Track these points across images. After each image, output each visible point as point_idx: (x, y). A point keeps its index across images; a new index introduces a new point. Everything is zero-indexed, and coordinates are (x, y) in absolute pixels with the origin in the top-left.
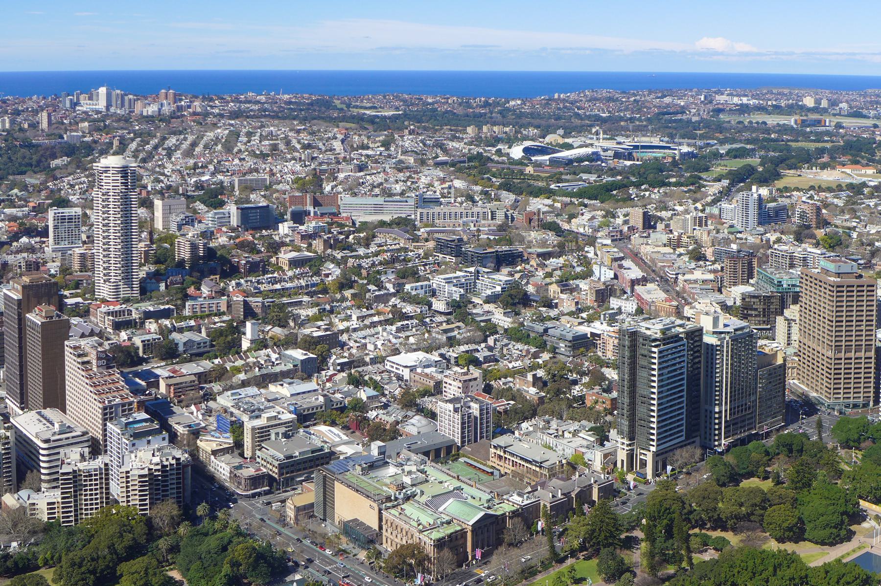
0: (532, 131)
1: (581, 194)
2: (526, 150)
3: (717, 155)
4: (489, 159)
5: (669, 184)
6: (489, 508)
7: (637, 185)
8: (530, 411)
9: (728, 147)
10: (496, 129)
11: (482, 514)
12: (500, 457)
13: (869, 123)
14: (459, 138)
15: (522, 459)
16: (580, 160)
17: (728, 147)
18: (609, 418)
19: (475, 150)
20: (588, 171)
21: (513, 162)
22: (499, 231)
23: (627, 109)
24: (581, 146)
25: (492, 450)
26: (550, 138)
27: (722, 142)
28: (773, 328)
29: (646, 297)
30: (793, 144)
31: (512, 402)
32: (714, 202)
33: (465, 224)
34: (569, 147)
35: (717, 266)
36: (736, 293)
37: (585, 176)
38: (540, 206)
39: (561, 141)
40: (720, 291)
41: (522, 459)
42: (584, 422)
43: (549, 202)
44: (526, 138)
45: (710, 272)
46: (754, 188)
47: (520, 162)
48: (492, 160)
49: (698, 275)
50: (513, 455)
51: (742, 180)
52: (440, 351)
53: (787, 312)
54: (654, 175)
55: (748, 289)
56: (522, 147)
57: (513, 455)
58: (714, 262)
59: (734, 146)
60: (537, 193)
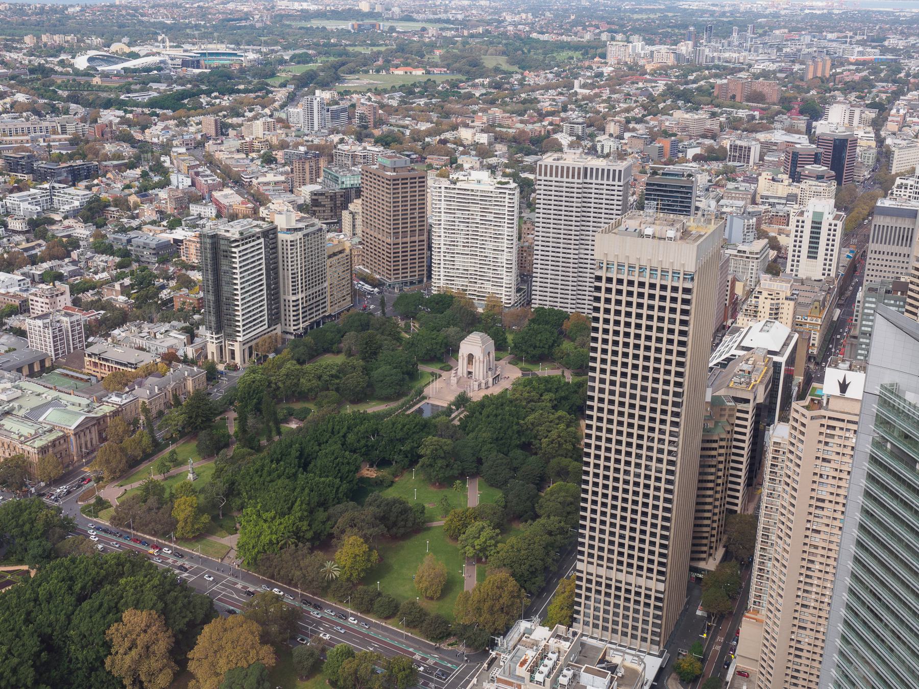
0: (97, 41)
1: (153, 104)
2: (90, 60)
3: (282, 62)
4: (52, 71)
5: (239, 91)
6: (89, 412)
7: (208, 93)
8: (121, 319)
9: (291, 52)
10: (56, 37)
11: (83, 418)
12: (95, 364)
13: (417, 26)
14: (16, 48)
15: (117, 363)
16: (148, 69)
17: (291, 52)
18: (196, 317)
19: (36, 61)
20: (157, 80)
21: (77, 72)
22: (72, 144)
23: (191, 16)
24: (147, 55)
25: (87, 359)
26: (115, 47)
27: (285, 48)
28: (339, 222)
29: (224, 201)
30: (350, 49)
31: (102, 312)
32: (282, 107)
33: (34, 140)
34: (135, 56)
35: (288, 168)
36: (306, 192)
37: (155, 86)
38: (112, 118)
39: (127, 50)
40: (291, 191)
41: (117, 363)
42: (174, 323)
43: (121, 113)
44: (90, 48)
45: (282, 174)
46: (318, 92)
47: (86, 73)
48: (56, 72)
49: (270, 177)
50: (107, 360)
51: (305, 85)
52: (22, 271)
53: (351, 207)
54: (223, 80)
55: (317, 187)
56: (86, 57)
57: (107, 360)
58: (284, 165)
59: (297, 52)
60: (108, 104)
